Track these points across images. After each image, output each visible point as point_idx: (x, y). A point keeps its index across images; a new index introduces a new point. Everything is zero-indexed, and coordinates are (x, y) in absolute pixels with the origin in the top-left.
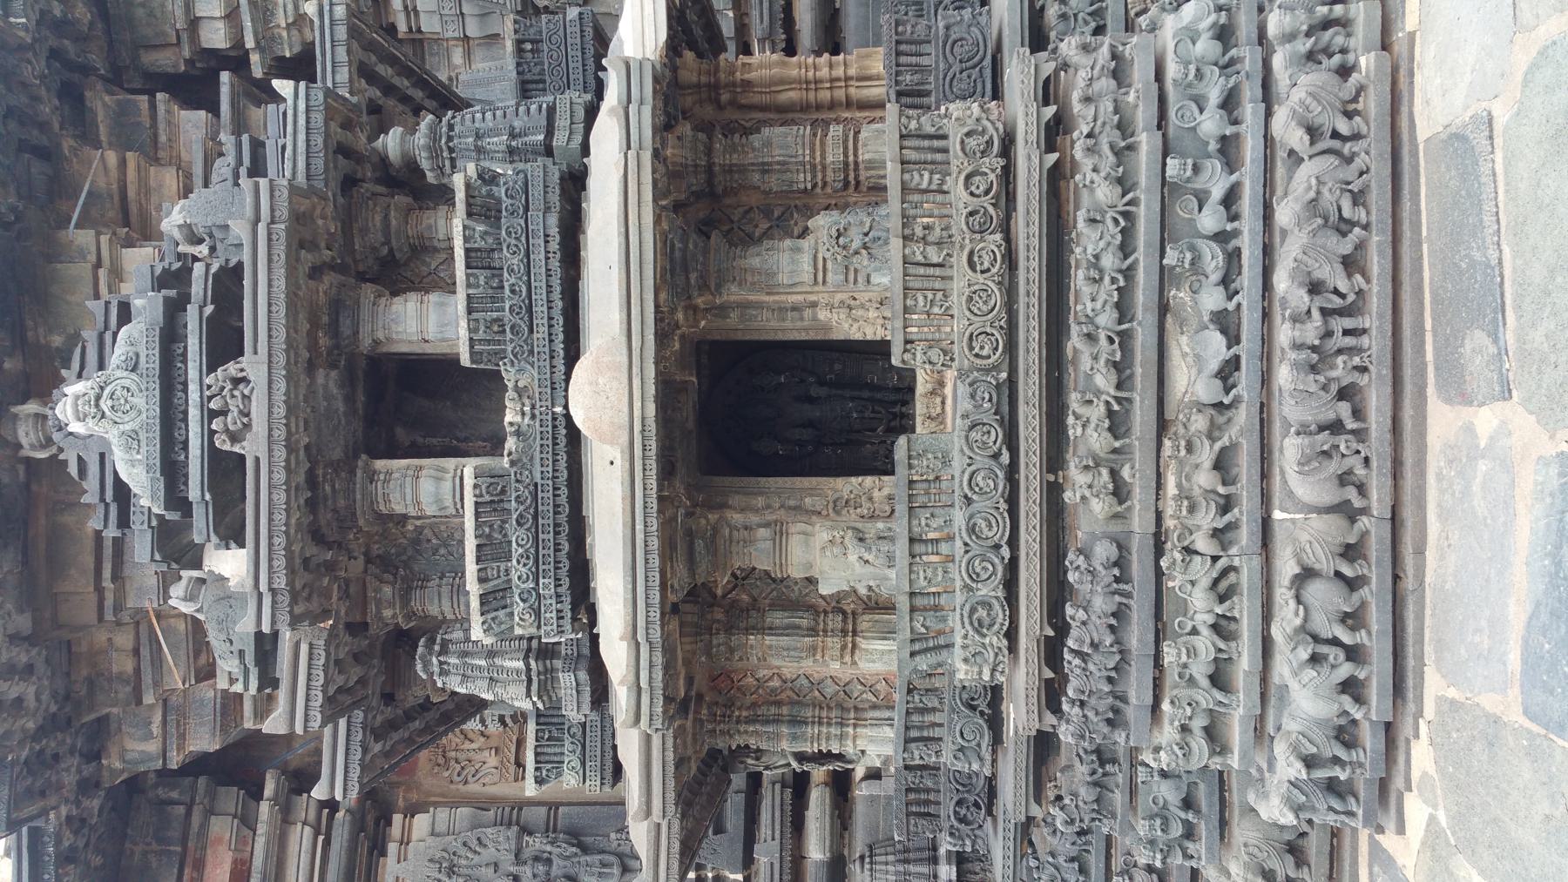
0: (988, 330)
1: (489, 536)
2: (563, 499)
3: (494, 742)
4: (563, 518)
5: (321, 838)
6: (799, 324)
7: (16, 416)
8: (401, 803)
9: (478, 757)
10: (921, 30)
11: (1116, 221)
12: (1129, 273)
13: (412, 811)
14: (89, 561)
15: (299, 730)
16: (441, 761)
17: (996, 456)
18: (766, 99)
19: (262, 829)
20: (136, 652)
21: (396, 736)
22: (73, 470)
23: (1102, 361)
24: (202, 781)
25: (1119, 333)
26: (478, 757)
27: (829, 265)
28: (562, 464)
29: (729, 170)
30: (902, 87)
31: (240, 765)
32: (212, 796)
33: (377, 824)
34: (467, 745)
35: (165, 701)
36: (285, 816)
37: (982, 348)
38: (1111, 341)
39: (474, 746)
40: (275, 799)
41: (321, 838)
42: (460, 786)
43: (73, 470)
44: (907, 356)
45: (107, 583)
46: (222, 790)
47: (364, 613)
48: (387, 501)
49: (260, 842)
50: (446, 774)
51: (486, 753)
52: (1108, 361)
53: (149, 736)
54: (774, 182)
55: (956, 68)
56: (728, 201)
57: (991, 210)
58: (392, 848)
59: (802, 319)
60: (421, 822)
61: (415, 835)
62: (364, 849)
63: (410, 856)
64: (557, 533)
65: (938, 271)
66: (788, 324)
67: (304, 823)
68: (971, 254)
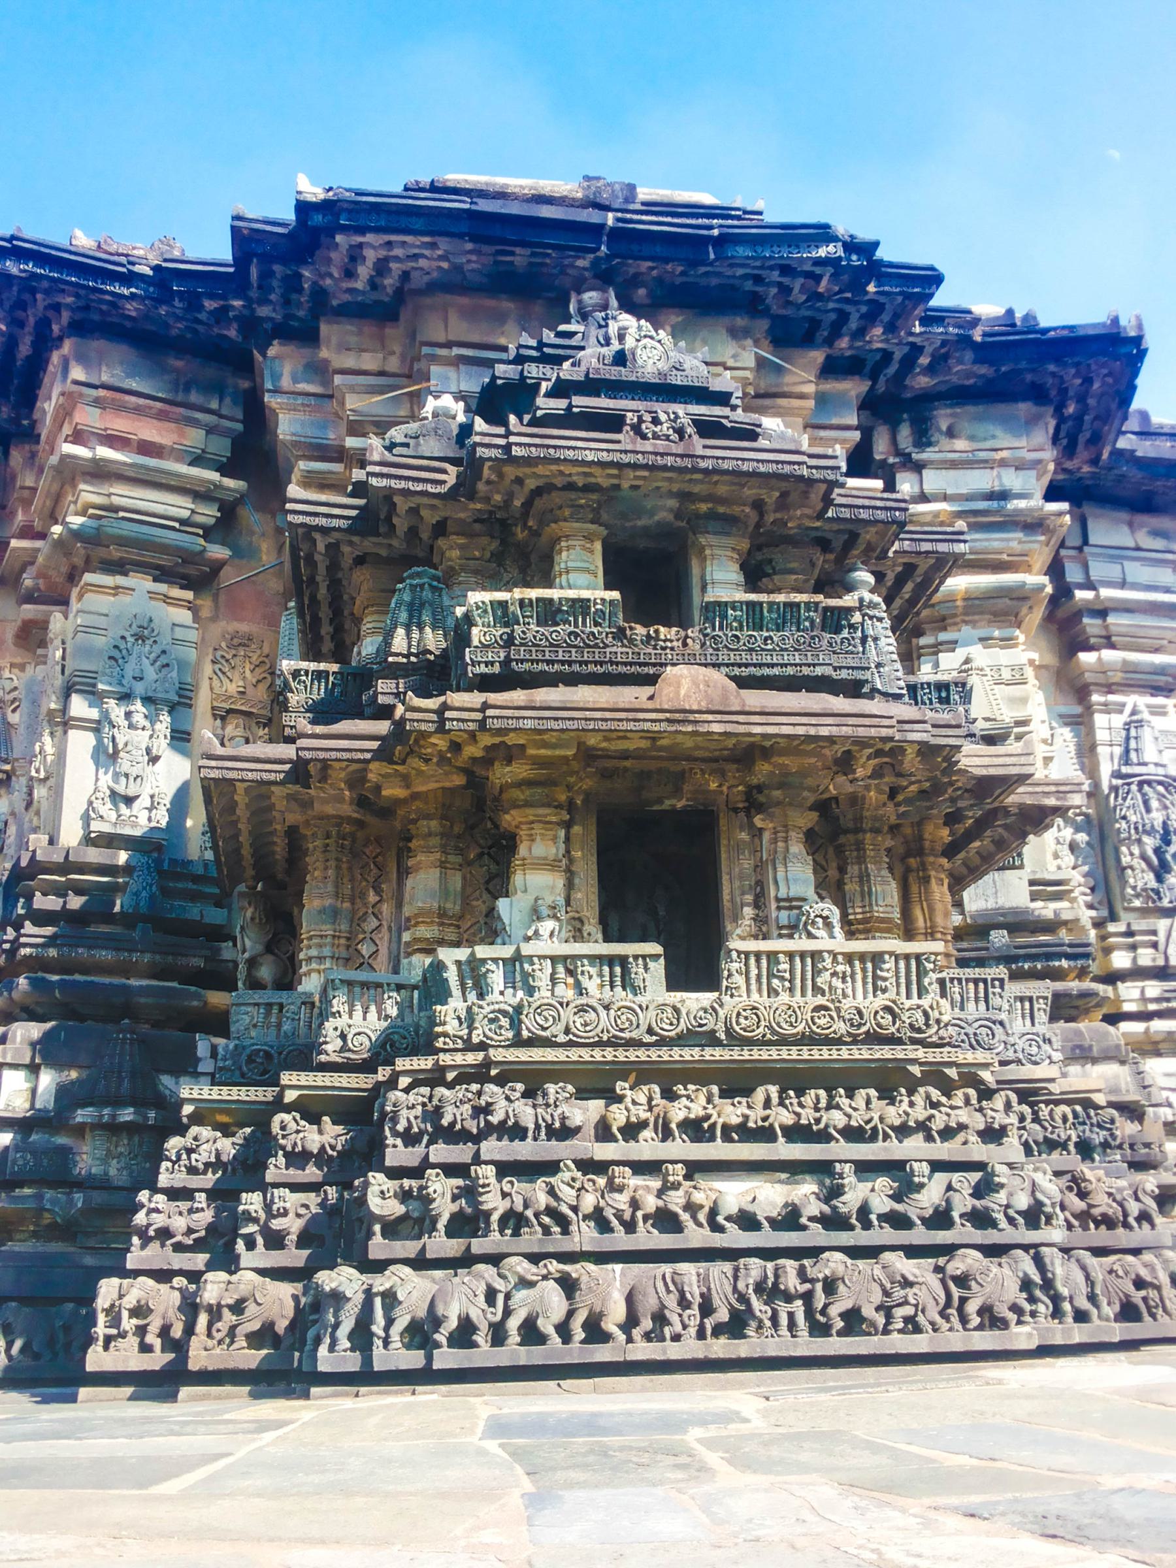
0: (763, 1023)
1: (559, 611)
2: (591, 668)
3: (250, 691)
4: (576, 668)
5: (177, 525)
6: (737, 892)
7: (604, 291)
8: (199, 602)
9: (236, 676)
10: (995, 1001)
11: (867, 1122)
12: (823, 1137)
13: (191, 607)
14: (475, 338)
15: (288, 506)
16: (236, 642)
17: (650, 1031)
18: (915, 897)
19: (195, 471)
20: (381, 373)
21: (322, 569)
22: (562, 328)
23: (747, 1112)
24: (239, 427)
25: (771, 1125)
26: (236, 676)
27: (796, 911)
28: (622, 669)
29: (859, 847)
30: (948, 985)
31: (253, 455)
32: (224, 433)
33: (184, 577)
34: (248, 666)
35: (331, 397)
36: (200, 494)
37: (746, 1018)
38: (764, 1119)
39: (248, 674)
40: (218, 487)
41: (177, 525)
42: (211, 657)
43: (562, 328)
44: (734, 955)
45: (456, 351)
46: (227, 442)
47: (457, 534)
48: (568, 548)
49: (184, 469)
50: (223, 645)
51: (241, 683)
52: (746, 1117)
53: (295, 380)
54: (851, 887)
55: (970, 1031)
56: (831, 850)
57: (864, 1029)
58: (162, 588)
59: (743, 894)
60: (185, 616)
61: (171, 609)
62: (165, 561)
63: (153, 602)
64: (563, 663)
65: (809, 983)
66: (737, 884)
67: (193, 511)
68: (826, 1009)
